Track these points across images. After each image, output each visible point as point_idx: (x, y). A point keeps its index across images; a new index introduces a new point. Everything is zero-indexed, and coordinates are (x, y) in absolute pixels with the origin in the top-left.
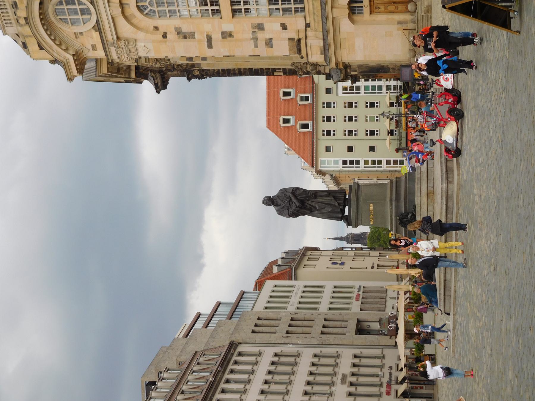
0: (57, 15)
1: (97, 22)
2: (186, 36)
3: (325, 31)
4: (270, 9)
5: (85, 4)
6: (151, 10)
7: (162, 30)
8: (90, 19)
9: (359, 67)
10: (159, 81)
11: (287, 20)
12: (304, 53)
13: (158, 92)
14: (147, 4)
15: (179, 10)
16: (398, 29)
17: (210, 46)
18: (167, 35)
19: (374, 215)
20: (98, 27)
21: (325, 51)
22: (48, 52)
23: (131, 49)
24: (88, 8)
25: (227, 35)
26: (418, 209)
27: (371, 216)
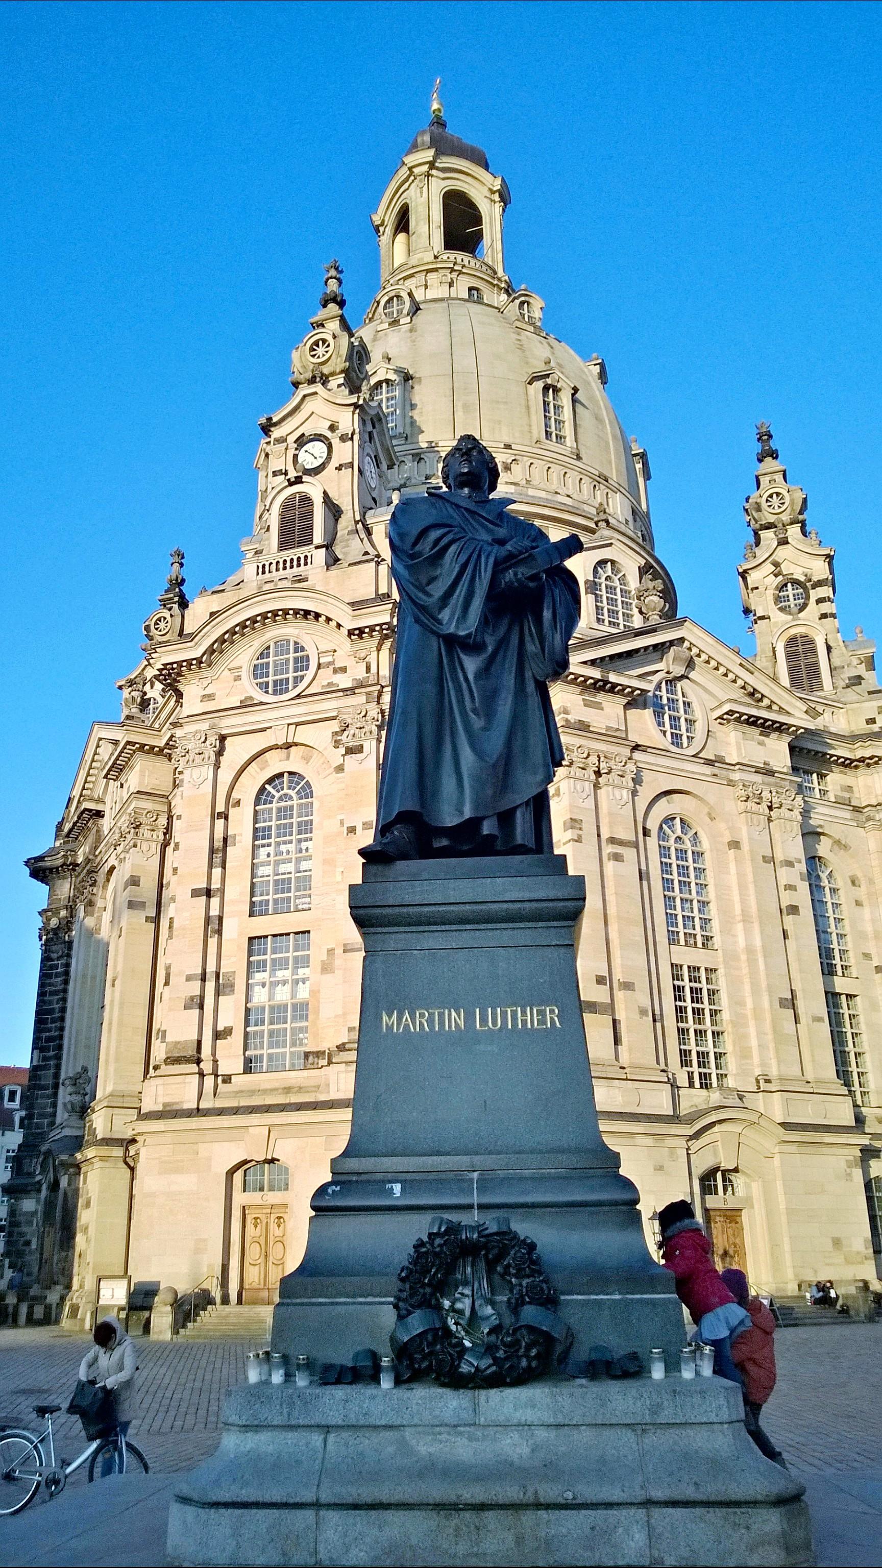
0: (275, 643)
1: (261, 703)
2: (218, 853)
3: (221, 1112)
4: (263, 1008)
5: (295, 687)
6: (273, 796)
7: (232, 812)
8: (267, 692)
9: (77, 1191)
10: (48, 864)
11: (237, 1038)
12: (165, 1069)
13: (27, 863)
14: (285, 791)
15: (269, 845)
16: (210, 1266)
17: (195, 893)
18: (223, 820)
19: (466, 1038)
20: (246, 705)
21: (169, 1113)
22: (206, 624)
23: (202, 756)
24: (287, 690)
25: (214, 926)
26: (621, 1399)
27: (455, 1019)
